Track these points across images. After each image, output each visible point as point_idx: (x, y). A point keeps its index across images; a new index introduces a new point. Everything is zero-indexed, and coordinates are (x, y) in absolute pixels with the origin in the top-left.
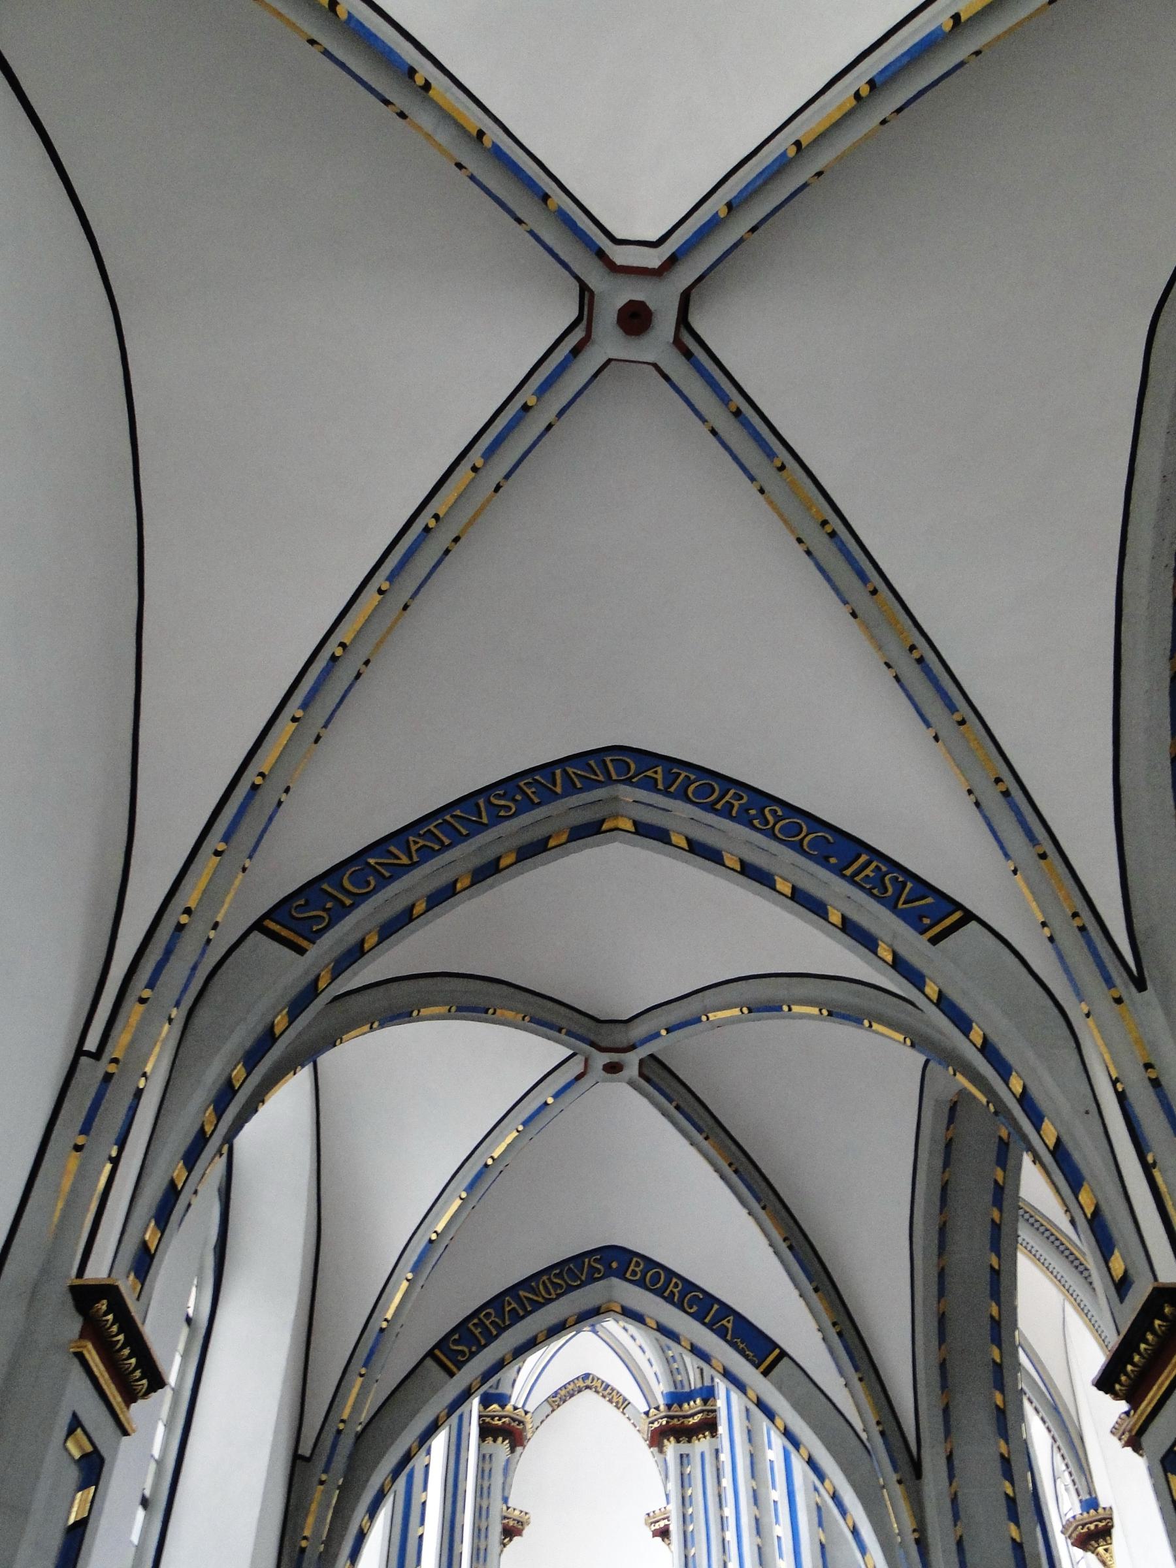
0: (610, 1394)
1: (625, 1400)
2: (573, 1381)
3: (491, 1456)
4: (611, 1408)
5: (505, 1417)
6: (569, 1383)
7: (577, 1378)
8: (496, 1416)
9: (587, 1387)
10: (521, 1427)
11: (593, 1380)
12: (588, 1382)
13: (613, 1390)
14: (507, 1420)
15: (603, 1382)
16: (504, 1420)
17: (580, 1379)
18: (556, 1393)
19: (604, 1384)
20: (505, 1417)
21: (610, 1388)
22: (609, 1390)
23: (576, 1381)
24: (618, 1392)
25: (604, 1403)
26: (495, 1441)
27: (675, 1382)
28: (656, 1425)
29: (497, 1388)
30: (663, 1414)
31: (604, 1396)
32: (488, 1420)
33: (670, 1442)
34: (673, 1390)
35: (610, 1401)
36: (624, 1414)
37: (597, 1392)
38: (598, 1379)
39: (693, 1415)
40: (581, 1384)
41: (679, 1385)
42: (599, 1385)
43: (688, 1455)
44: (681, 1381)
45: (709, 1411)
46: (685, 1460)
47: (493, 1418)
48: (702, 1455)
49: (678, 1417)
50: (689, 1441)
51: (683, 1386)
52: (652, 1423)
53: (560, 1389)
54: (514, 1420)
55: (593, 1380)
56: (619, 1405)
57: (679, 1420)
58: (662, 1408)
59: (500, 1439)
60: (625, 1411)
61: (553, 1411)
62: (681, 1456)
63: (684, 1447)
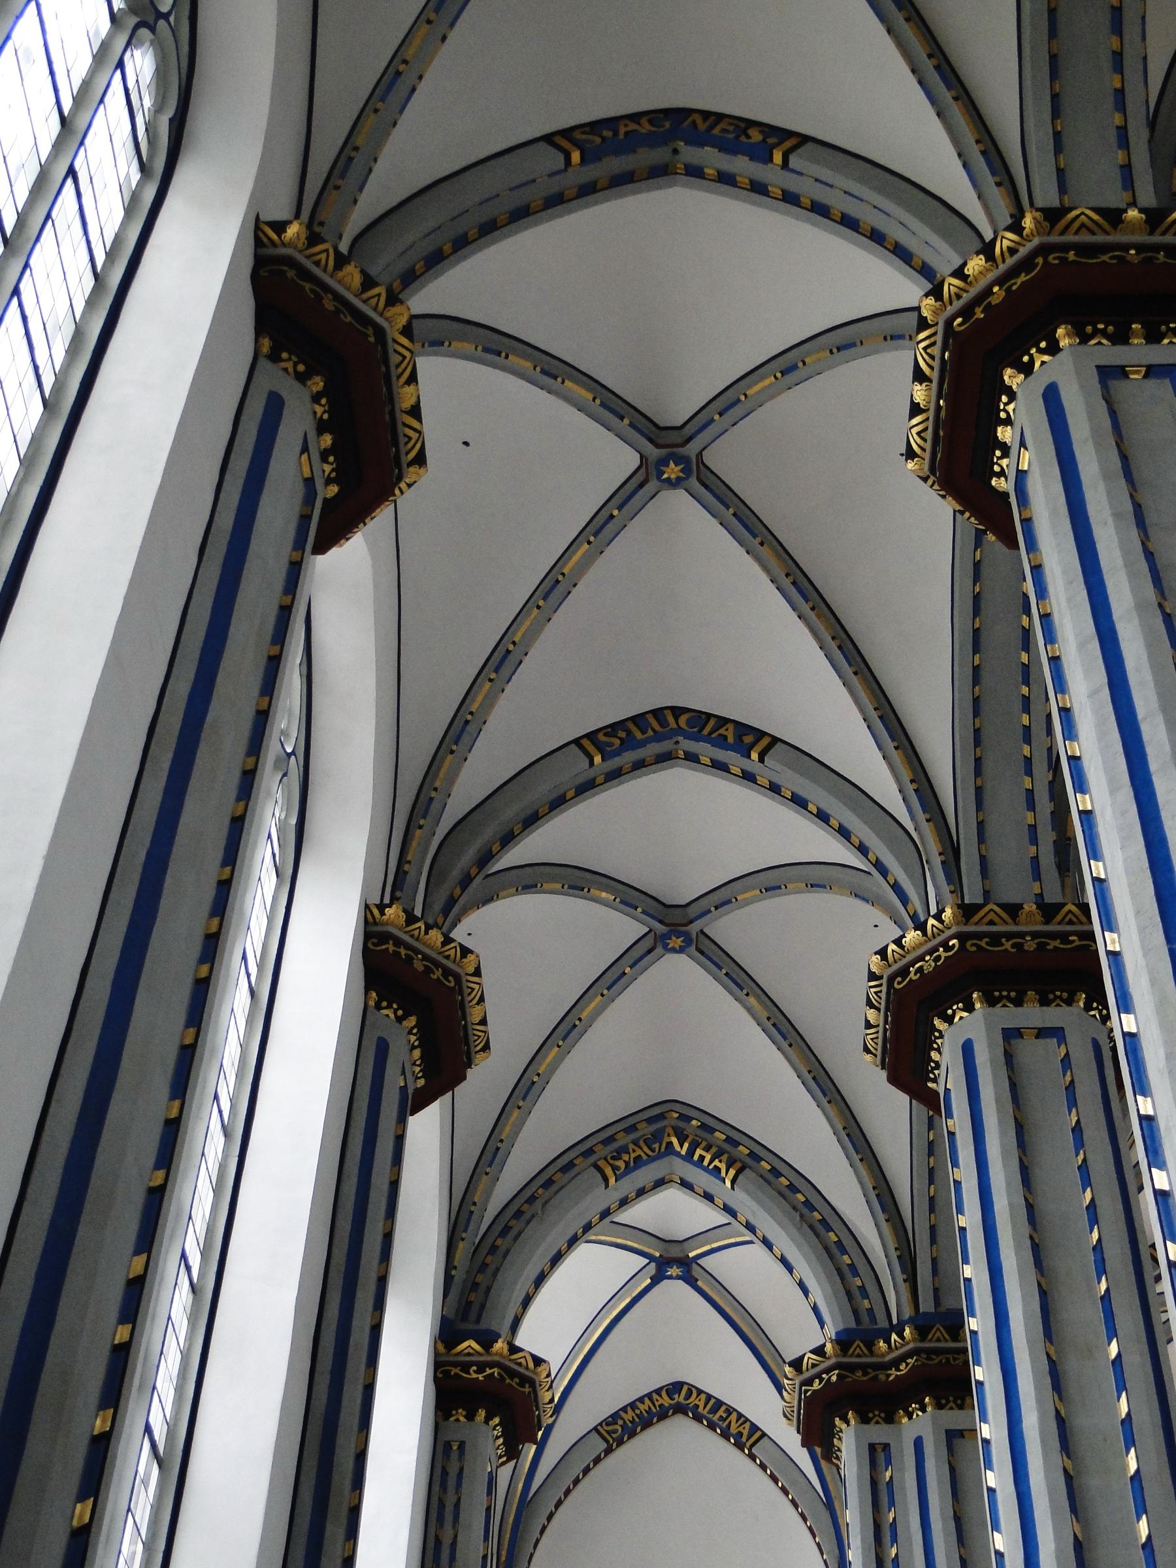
0: (722, 1419)
1: (754, 1428)
2: (649, 1395)
3: (462, 1445)
4: (726, 1451)
5: (492, 1365)
6: (641, 1400)
7: (658, 1391)
8: (472, 1364)
9: (680, 1409)
10: (527, 1389)
11: (689, 1394)
12: (680, 1398)
13: (730, 1410)
14: (496, 1371)
15: (709, 1397)
16: (489, 1371)
17: (664, 1393)
18: (615, 1417)
19: (712, 1401)
20: (492, 1365)
21: (723, 1408)
22: (721, 1413)
23: (655, 1396)
24: (740, 1415)
25: (713, 1440)
26: (470, 1417)
27: (855, 1312)
28: (816, 1385)
29: (478, 1320)
30: (833, 1361)
31: (712, 1426)
32: (454, 1371)
33: (848, 1424)
34: (852, 1324)
35: (725, 1435)
36: (752, 1457)
37: (698, 1418)
38: (700, 1392)
39: (896, 1363)
40: (666, 1401)
41: (865, 1318)
42: (701, 1404)
43: (886, 1447)
44: (870, 1311)
45: (930, 1352)
46: (881, 1457)
47: (466, 1367)
48: (918, 1443)
49: (864, 1367)
50: (890, 1419)
51: (873, 1319)
52: (809, 1382)
53: (624, 1409)
54: (512, 1374)
55: (689, 1394)
56: (744, 1439)
57: (865, 1374)
58: (829, 1348)
59: (482, 1414)
60: (754, 1450)
61: (609, 1451)
62: (872, 1448)
63: (878, 1432)
